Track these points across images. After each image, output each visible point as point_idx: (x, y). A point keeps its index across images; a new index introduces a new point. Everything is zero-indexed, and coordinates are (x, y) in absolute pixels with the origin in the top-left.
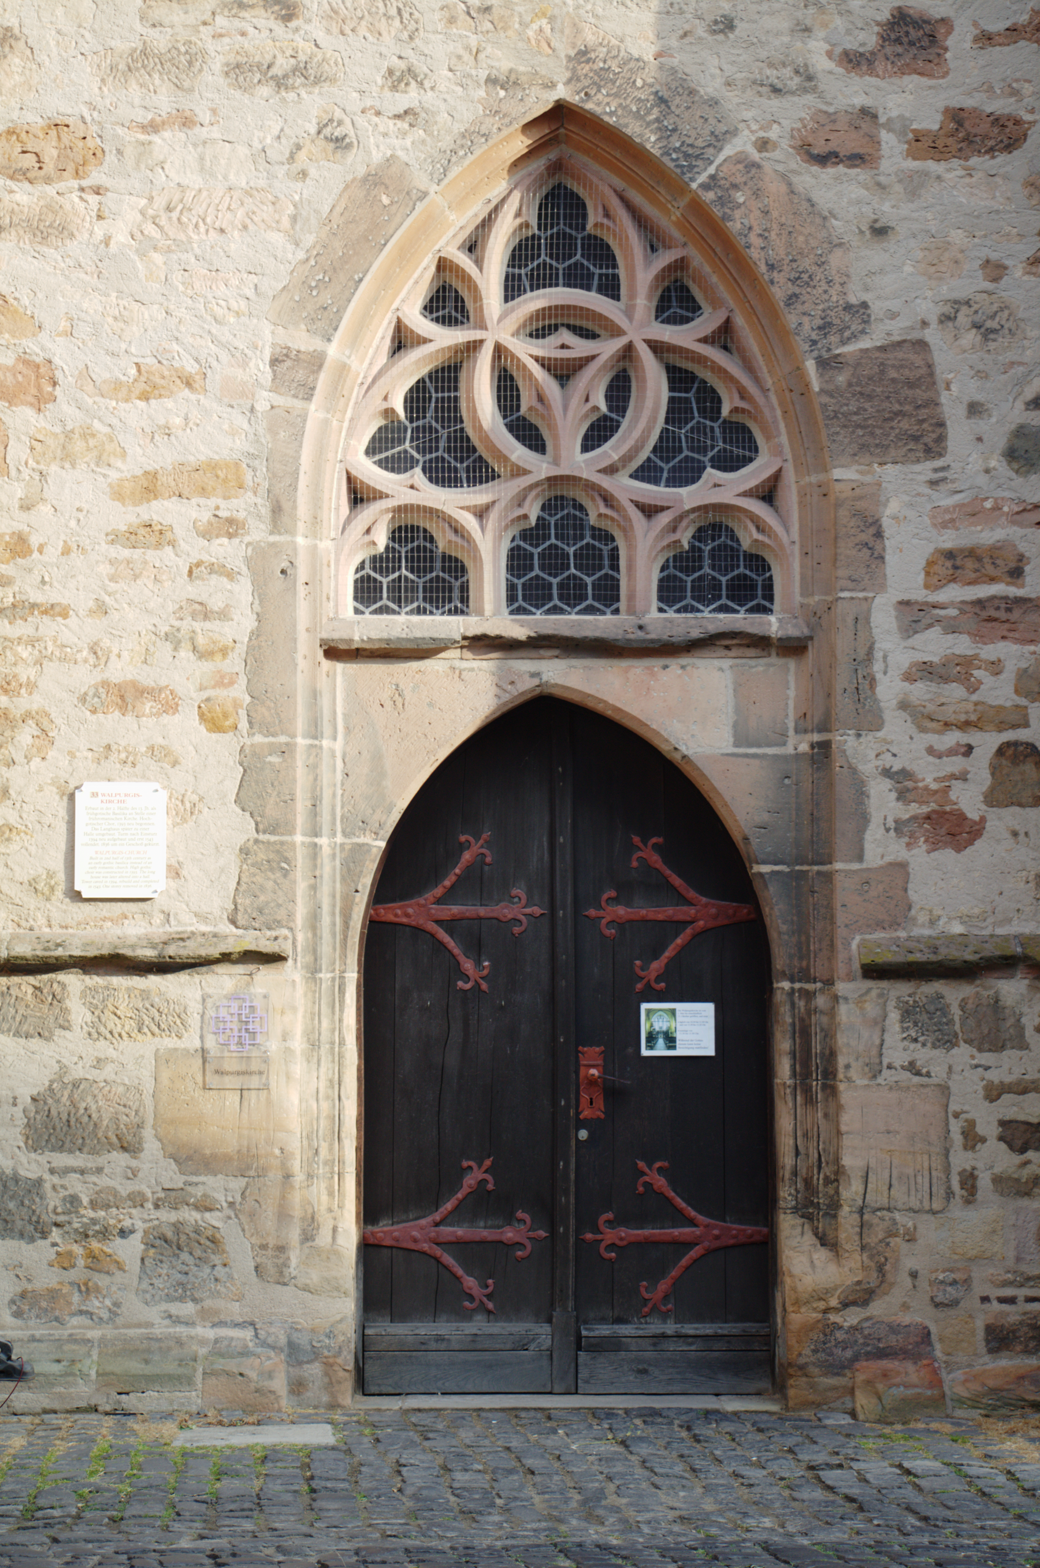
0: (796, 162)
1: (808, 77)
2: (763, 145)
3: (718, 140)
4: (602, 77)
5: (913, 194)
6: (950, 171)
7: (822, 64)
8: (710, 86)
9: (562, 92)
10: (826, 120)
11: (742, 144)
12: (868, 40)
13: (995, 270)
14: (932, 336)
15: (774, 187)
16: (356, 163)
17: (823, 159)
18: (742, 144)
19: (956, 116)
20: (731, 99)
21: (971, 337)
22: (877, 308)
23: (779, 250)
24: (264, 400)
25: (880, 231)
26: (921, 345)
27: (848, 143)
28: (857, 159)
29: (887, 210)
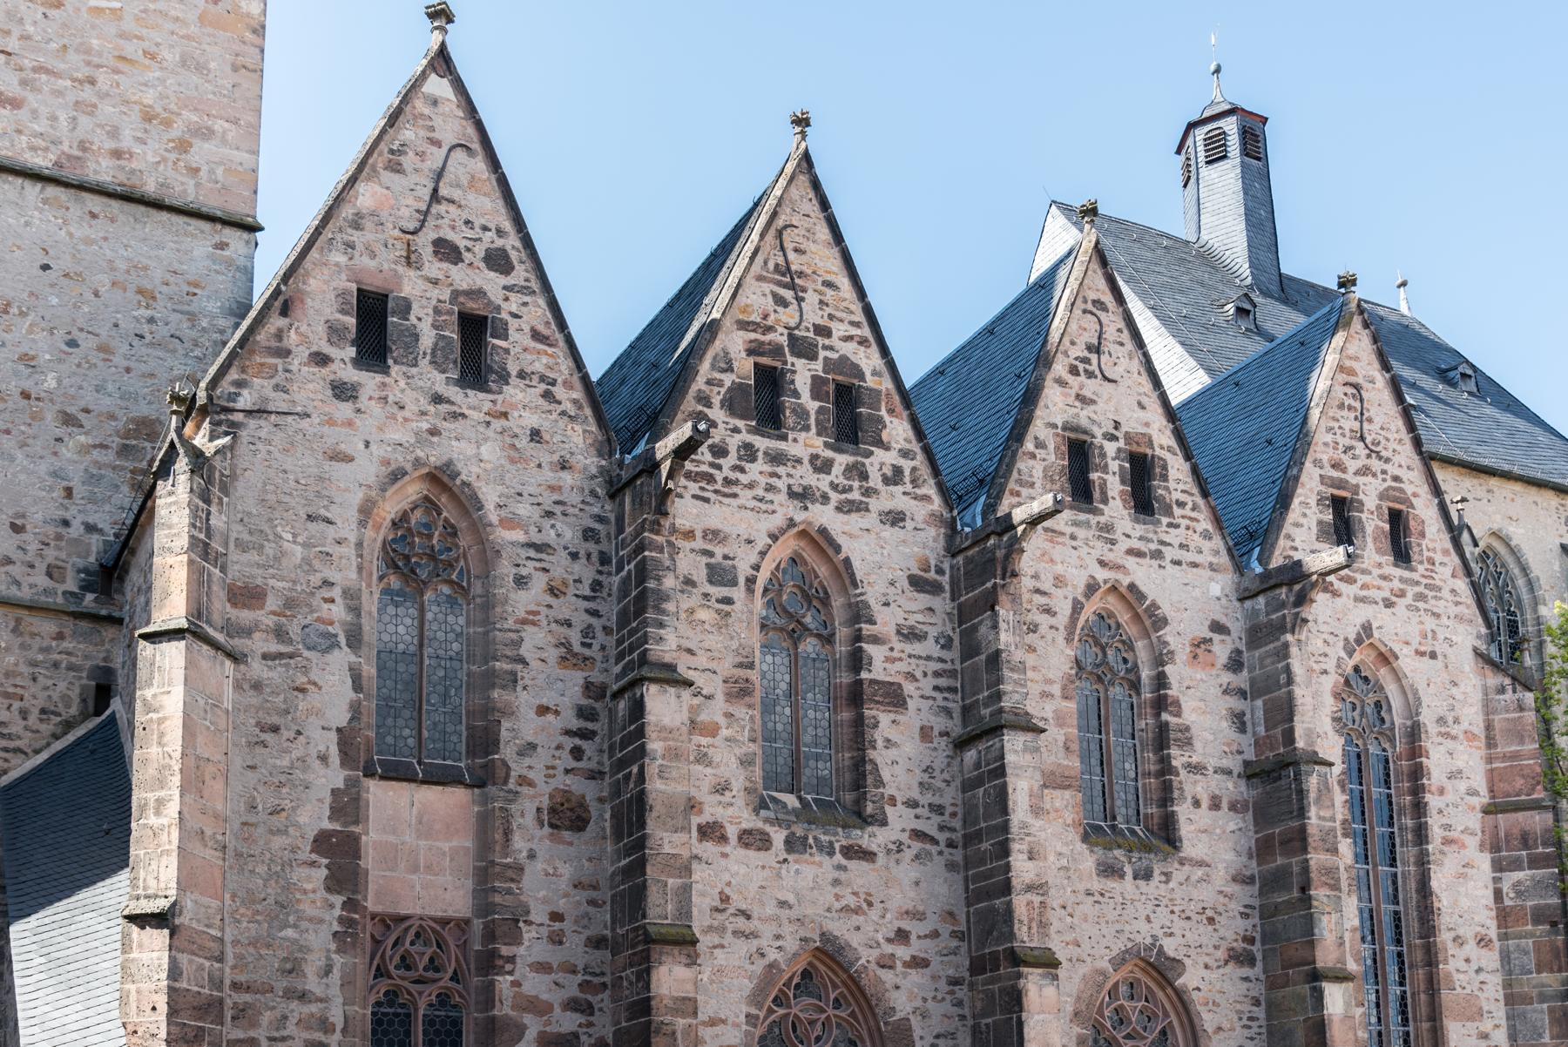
0: (876, 967)
2: (868, 962)
3: (858, 959)
6: (913, 971)
8: (855, 945)
10: (883, 956)
12: (892, 935)
13: (925, 1000)
14: (911, 1017)
15: (871, 974)
16: (766, 961)
17: (883, 967)
19: (914, 957)
20: (860, 949)
21: (920, 1018)
22: (898, 1009)
23: (873, 991)
24: (744, 1027)
25: (897, 988)
26: (908, 1020)
28: (891, 967)
29: (898, 981)
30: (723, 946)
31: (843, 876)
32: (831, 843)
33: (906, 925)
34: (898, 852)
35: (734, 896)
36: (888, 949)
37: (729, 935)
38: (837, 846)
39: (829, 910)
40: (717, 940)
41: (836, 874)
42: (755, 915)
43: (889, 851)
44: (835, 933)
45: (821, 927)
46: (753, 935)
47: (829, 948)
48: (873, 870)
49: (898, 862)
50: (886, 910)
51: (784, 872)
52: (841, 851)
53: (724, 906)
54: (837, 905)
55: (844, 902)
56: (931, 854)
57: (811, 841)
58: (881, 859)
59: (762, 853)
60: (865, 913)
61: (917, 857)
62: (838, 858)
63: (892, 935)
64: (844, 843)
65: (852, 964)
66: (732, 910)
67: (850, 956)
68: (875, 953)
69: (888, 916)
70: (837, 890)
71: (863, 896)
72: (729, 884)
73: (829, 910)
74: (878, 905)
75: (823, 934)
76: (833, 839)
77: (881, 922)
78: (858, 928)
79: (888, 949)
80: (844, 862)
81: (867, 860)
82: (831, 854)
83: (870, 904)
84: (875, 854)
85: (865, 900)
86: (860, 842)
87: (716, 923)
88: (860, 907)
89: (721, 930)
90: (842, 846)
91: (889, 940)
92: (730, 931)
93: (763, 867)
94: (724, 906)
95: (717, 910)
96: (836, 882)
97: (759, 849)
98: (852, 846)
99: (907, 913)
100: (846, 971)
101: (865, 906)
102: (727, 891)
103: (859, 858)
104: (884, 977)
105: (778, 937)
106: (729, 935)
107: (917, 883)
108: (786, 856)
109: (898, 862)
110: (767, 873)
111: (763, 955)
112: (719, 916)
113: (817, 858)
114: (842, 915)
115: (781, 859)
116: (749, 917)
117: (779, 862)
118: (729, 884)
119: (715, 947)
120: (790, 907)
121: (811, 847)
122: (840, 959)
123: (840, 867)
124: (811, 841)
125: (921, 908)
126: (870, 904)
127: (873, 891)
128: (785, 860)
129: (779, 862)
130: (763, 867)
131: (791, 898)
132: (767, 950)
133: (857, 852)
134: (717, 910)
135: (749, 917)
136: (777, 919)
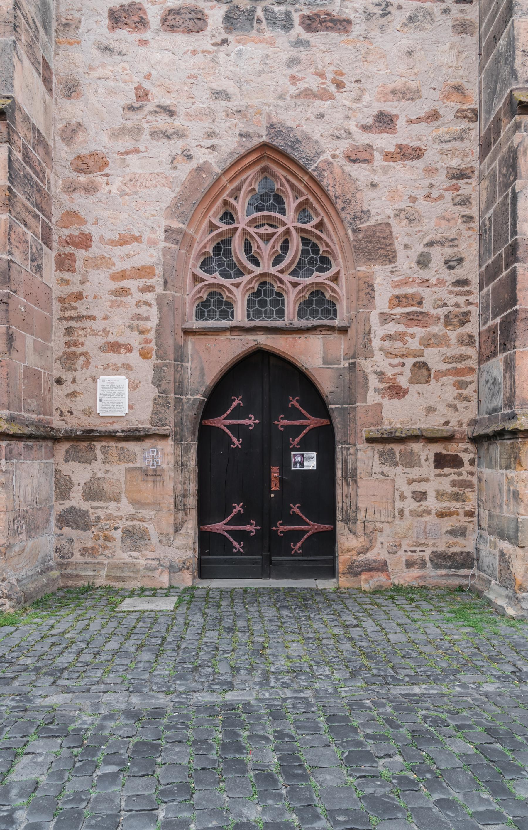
0: (345, 162)
1: (349, 133)
2: (334, 156)
3: (318, 155)
4: (279, 134)
5: (385, 173)
6: (398, 165)
7: (354, 129)
8: (316, 136)
9: (264, 138)
11: (327, 156)
12: (370, 121)
15: (338, 171)
16: (194, 164)
17: (354, 161)
18: (327, 156)
19: (400, 147)
20: (323, 141)
23: (339, 193)
25: (374, 186)
27: (363, 155)
28: (366, 161)
29: (376, 179)
30: (137, 151)
31: (303, 54)
32: (288, 14)
33: (390, 108)
34: (384, 15)
35: (155, 91)
36: (365, 138)
37: (146, 136)
38: (296, 17)
39: (281, 97)
40: (130, 144)
41: (294, 52)
42: (181, 110)
43: (369, 16)
44: (288, 124)
45: (269, 117)
46: (180, 134)
47: (279, 143)
48: (347, 42)
49: (382, 28)
50: (363, 91)
51: (222, 56)
52: (302, 23)
53: (140, 103)
54: (293, 90)
55: (302, 85)
56: (431, 14)
57: (260, 13)
58: (357, 30)
59: (194, 37)
60: (331, 97)
61: (411, 20)
62: (298, 30)
63: (370, 121)
64: (306, 12)
65: (310, 160)
66: (150, 107)
67: (308, 150)
68: (344, 145)
69: (366, 98)
70: (294, 71)
71: (330, 76)
72: (148, 77)
73: (281, 97)
74: (350, 85)
75: (272, 126)
76: (291, 9)
77: (354, 106)
78: (321, 116)
79: (365, 138)
80: (306, 36)
81: (339, 30)
82: (288, 26)
83: (340, 85)
84: (349, 22)
85: (334, 81)
86: (329, 9)
87: (129, 124)
88: (326, 90)
89: (136, 131)
90: (303, 17)
91: (365, 128)
92: (147, 132)
93: (194, 53)
94: (140, 103)
95: (131, 108)
96: (293, 62)
97: (190, 31)
98: (318, 15)
99: (393, 92)
100: (305, 171)
101: (333, 88)
102: (146, 85)
103: (327, 29)
104: (354, 175)
105: (211, 135)
106: (146, 136)
107: (410, 54)
108: (225, 36)
109: (382, 28)
110: (199, 59)
111: (189, 157)
112: (135, 117)
113: (268, 35)
114: (299, 101)
115: (219, 40)
116: (172, 114)
117: (215, 44)
118: (148, 77)
119: (127, 153)
120: (228, 97)
121: (259, 21)
122: (295, 155)
123: (299, 43)
124: (260, 13)
125: (414, 85)
126: (340, 85)
127: (345, 69)
128: (225, 42)
129: (215, 44)
130: (194, 53)
131: (231, 87)
132: (195, 152)
133: (325, 21)
134: (131, 108)
135: (172, 114)
136: (210, 113)
